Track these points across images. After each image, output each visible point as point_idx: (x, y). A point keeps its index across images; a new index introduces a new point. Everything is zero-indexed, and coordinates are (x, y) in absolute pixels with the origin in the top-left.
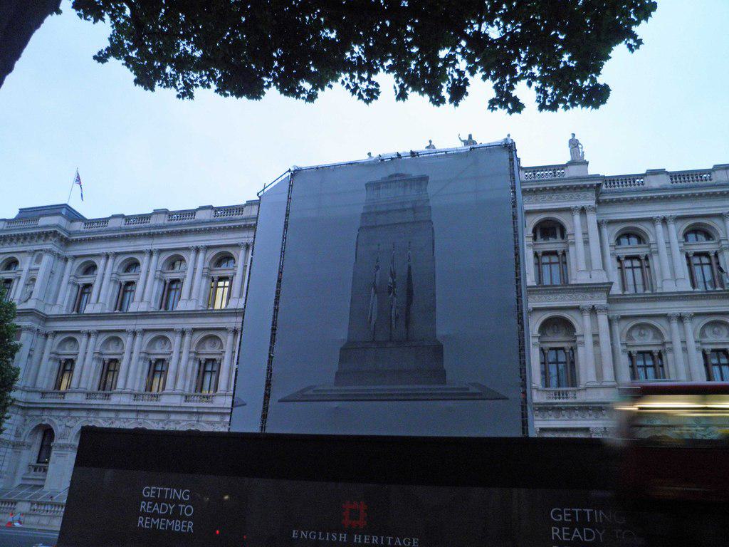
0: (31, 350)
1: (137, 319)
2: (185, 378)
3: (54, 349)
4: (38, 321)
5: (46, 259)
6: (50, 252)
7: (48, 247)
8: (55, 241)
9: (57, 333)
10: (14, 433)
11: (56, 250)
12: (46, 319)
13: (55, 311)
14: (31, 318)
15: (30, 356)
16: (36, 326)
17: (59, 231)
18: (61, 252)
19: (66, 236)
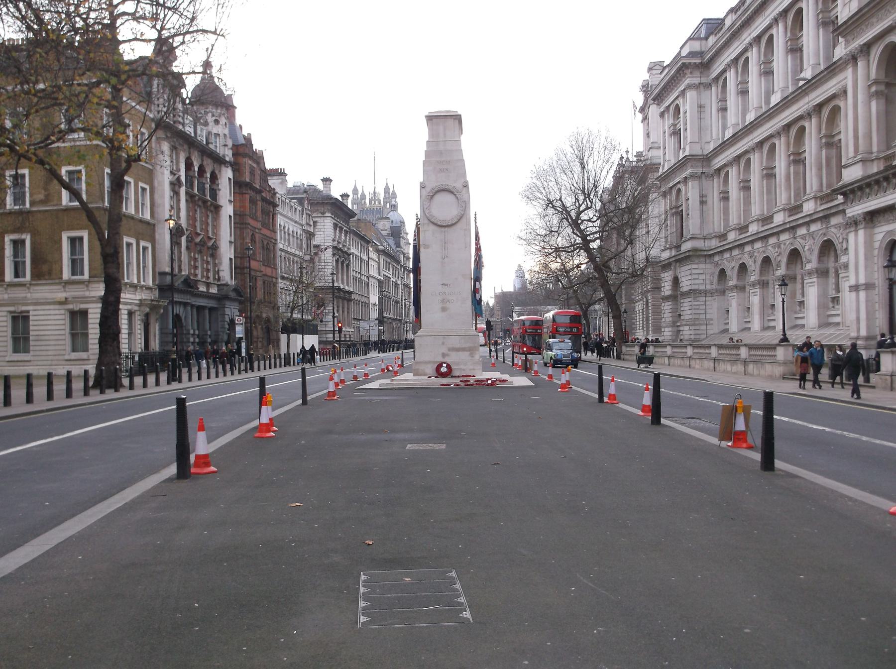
0: (702, 196)
1: (751, 132)
2: (788, 187)
3: (721, 188)
4: (700, 164)
5: (689, 94)
6: (689, 87)
7: (688, 81)
8: (691, 73)
9: (719, 170)
10: (708, 282)
11: (696, 81)
12: (706, 159)
13: (711, 147)
14: (690, 164)
15: (703, 203)
16: (699, 170)
17: (687, 61)
18: (704, 80)
19: (698, 61)
